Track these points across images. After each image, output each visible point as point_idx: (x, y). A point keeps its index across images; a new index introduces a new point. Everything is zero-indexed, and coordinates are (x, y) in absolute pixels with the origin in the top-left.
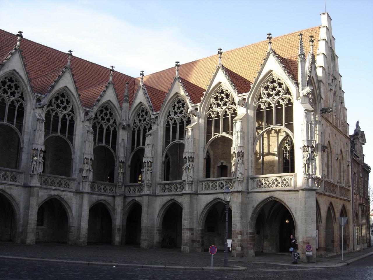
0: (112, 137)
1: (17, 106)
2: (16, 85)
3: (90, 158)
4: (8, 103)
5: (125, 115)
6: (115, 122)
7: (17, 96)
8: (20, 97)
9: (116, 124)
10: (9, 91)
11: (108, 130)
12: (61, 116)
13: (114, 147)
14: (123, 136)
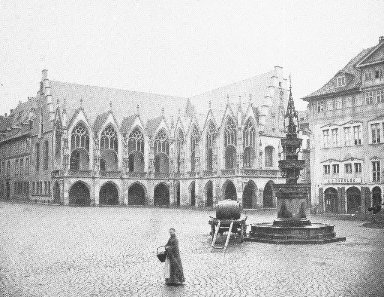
0: (167, 147)
1: (114, 139)
2: (112, 129)
3: (152, 161)
4: (109, 139)
5: (172, 134)
6: (167, 139)
7: (113, 135)
8: (115, 135)
9: (168, 140)
10: (109, 133)
11: (164, 144)
12: (137, 141)
13: (168, 153)
14: (173, 147)
